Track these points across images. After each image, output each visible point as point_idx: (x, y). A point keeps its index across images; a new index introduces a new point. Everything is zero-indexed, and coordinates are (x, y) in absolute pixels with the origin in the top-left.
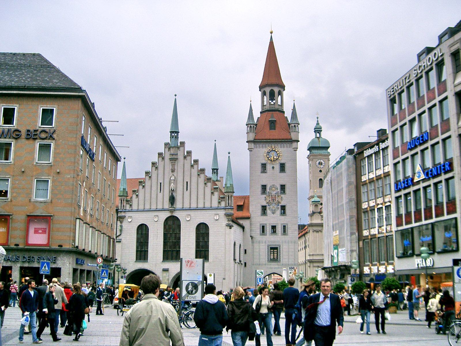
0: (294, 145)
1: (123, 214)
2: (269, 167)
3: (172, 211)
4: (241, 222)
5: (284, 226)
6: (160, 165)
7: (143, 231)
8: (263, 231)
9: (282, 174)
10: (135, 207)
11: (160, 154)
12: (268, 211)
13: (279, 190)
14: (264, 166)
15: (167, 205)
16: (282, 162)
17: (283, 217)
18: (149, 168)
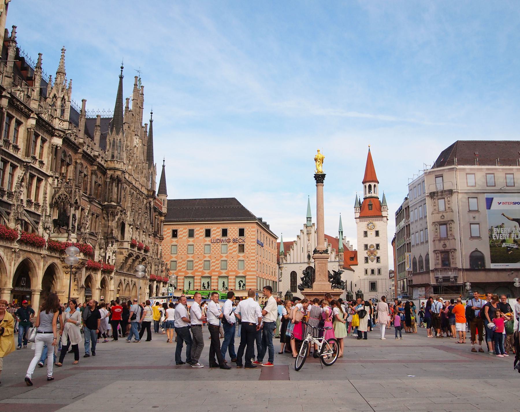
0: (385, 219)
1: (282, 265)
2: (369, 233)
3: (308, 263)
4: (352, 267)
5: (379, 270)
6: (302, 237)
7: (293, 275)
8: (366, 273)
9: (377, 238)
10: (288, 262)
11: (301, 231)
12: (369, 261)
13: (375, 247)
14: (366, 233)
15: (306, 260)
16: (377, 230)
17: (378, 264)
18: (299, 233)
